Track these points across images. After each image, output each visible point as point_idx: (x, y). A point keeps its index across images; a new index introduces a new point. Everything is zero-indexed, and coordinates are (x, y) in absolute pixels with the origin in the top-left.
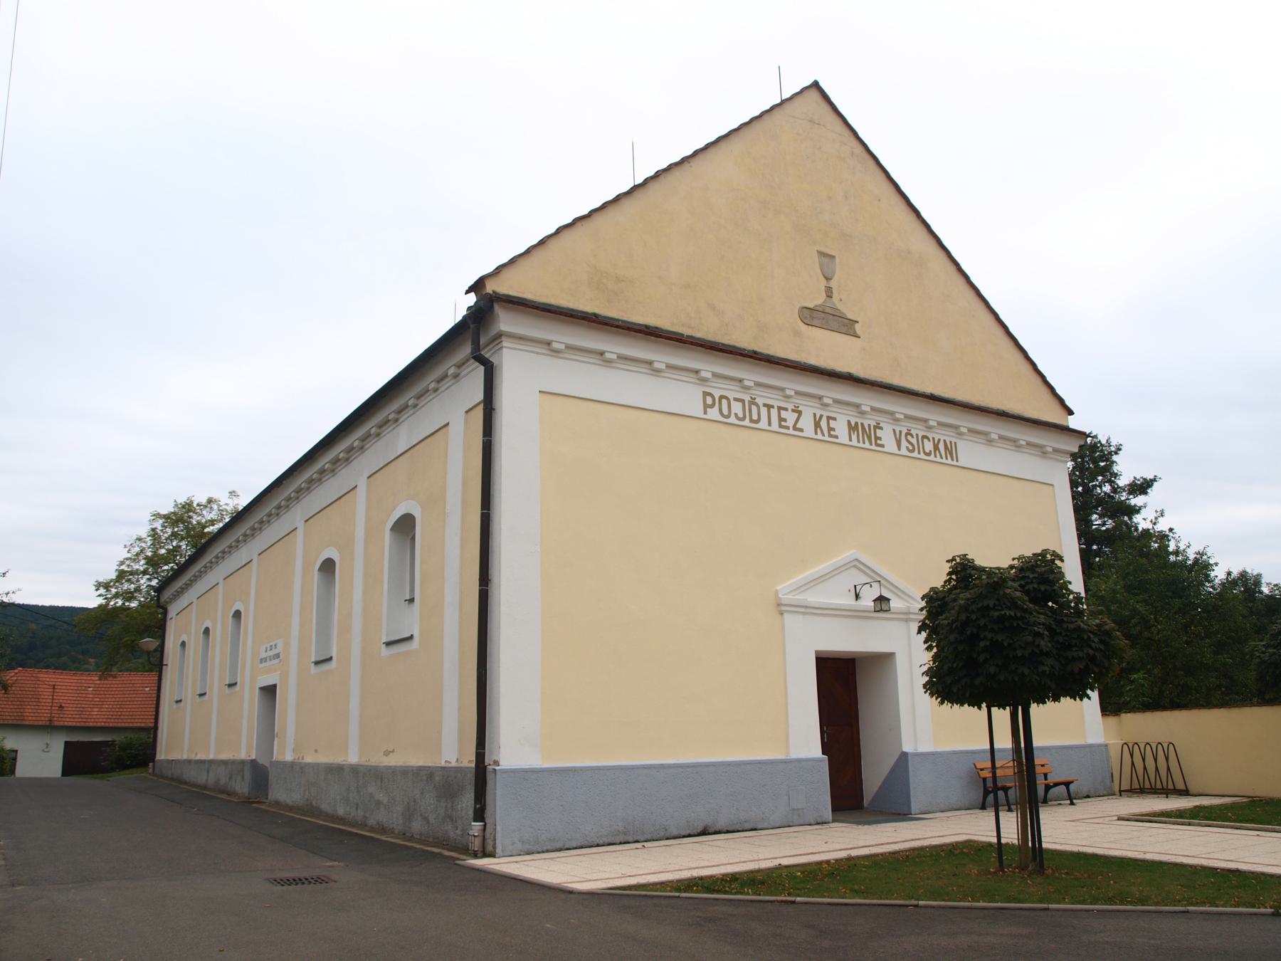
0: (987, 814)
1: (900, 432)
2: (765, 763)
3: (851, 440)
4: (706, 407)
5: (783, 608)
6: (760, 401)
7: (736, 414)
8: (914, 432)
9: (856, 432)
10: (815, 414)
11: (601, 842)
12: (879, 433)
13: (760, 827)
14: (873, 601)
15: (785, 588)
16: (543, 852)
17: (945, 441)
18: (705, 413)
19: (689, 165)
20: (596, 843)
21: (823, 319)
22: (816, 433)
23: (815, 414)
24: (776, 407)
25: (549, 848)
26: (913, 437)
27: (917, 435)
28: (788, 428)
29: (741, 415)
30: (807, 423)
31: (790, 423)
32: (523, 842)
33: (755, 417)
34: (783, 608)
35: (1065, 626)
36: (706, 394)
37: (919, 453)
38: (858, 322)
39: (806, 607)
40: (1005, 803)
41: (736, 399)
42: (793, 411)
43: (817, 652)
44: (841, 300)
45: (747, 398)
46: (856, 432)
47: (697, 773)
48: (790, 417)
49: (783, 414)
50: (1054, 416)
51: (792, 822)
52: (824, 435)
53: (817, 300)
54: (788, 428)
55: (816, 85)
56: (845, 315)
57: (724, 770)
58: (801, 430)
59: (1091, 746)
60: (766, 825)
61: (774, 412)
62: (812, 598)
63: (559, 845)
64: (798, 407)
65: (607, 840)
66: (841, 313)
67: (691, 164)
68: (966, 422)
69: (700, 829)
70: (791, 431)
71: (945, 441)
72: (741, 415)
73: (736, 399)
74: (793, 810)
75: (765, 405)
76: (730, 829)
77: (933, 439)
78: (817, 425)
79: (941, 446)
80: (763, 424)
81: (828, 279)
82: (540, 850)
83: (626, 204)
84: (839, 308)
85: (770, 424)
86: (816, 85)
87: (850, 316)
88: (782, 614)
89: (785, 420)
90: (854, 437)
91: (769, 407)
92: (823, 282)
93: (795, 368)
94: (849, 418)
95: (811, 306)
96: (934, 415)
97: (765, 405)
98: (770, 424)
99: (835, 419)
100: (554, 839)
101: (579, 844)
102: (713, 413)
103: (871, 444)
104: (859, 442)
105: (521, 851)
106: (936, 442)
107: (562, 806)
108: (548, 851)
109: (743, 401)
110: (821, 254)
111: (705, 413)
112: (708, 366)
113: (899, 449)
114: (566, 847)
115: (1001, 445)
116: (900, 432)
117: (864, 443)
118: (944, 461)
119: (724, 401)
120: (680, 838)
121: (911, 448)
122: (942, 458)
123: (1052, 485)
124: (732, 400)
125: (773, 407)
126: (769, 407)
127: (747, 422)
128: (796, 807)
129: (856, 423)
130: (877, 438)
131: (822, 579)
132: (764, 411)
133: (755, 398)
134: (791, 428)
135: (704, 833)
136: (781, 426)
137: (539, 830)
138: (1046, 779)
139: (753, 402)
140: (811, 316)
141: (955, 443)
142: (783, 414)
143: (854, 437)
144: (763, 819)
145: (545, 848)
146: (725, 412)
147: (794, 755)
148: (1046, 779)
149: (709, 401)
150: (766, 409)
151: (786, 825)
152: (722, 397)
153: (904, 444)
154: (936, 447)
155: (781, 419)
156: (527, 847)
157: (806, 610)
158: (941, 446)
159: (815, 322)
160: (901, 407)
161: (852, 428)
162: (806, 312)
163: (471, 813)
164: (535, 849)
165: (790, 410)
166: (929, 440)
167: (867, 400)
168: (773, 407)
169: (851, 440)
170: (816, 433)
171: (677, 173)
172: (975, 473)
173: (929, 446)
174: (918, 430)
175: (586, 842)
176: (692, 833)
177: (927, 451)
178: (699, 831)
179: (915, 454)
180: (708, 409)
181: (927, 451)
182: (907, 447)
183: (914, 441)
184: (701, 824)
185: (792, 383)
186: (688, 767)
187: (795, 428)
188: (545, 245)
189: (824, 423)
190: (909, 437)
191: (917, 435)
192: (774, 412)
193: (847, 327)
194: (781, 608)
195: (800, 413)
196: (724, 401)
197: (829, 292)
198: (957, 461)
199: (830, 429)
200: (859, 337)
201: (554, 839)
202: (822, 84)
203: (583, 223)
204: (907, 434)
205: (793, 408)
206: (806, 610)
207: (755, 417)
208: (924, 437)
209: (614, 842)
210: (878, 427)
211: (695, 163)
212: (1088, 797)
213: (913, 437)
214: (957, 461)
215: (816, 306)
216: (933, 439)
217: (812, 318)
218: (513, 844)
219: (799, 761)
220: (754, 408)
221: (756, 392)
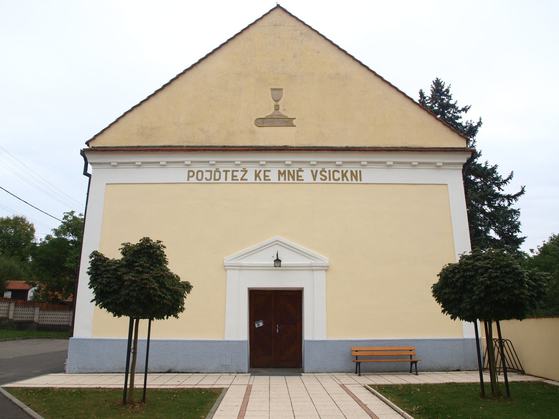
0: (410, 377)
2: (207, 342)
3: (279, 180)
4: (189, 177)
5: (226, 268)
6: (221, 170)
8: (327, 170)
9: (283, 176)
11: (115, 372)
12: (300, 173)
13: (201, 372)
14: (274, 261)
15: (228, 260)
16: (87, 373)
18: (188, 180)
19: (196, 68)
20: (112, 372)
21: (271, 122)
24: (231, 171)
25: (90, 372)
27: (329, 171)
28: (238, 180)
29: (209, 178)
30: (250, 176)
31: (239, 177)
32: (79, 368)
33: (217, 177)
34: (226, 268)
35: (460, 269)
36: (189, 171)
38: (295, 119)
39: (242, 266)
40: (415, 371)
41: (206, 171)
42: (242, 171)
43: (248, 288)
44: (285, 110)
45: (213, 169)
46: (283, 176)
47: (167, 344)
48: (239, 175)
49: (235, 174)
51: (221, 371)
54: (238, 180)
55: (278, 6)
56: (287, 117)
57: (183, 344)
58: (246, 180)
59: (464, 340)
60: (205, 371)
62: (245, 262)
63: (94, 371)
64: (245, 169)
65: (118, 371)
66: (285, 116)
67: (197, 67)
68: (364, 158)
69: (167, 370)
70: (240, 181)
72: (209, 178)
73: (206, 171)
74: (223, 365)
75: (224, 171)
76: (184, 371)
78: (257, 175)
80: (223, 179)
81: (276, 101)
82: (86, 372)
83: (160, 94)
84: (283, 114)
85: (226, 179)
86: (278, 6)
87: (289, 117)
88: (226, 270)
90: (282, 178)
91: (226, 172)
92: (274, 103)
93: (240, 150)
94: (279, 169)
95: (264, 117)
96: (339, 158)
97: (224, 171)
99: (269, 171)
100: (93, 368)
101: (104, 371)
102: (193, 180)
103: (294, 180)
105: (77, 372)
106: (344, 173)
107: (97, 355)
108: (89, 373)
110: (273, 90)
111: (188, 180)
112: (188, 159)
114: (98, 372)
115: (420, 167)
118: (350, 181)
120: (155, 373)
121: (323, 178)
123: (447, 184)
124: (204, 172)
125: (229, 171)
127: (212, 181)
128: (224, 364)
131: (257, 251)
132: (223, 174)
133: (218, 169)
135: (169, 372)
136: (233, 180)
137: (86, 364)
138: (411, 358)
139: (217, 170)
140: (261, 122)
141: (360, 171)
142: (235, 174)
144: (203, 368)
145: (88, 372)
146: (200, 177)
147: (227, 338)
148: (411, 358)
149: (191, 174)
150: (225, 173)
151: (218, 372)
152: (198, 171)
153: (319, 176)
154: (344, 175)
155: (233, 176)
156: (80, 370)
157: (241, 268)
159: (265, 124)
160: (313, 158)
162: (260, 121)
164: (83, 371)
165: (240, 171)
167: (288, 158)
168: (229, 171)
169: (279, 180)
170: (256, 180)
171: (189, 73)
172: (377, 185)
173: (338, 175)
174: (330, 168)
175: (107, 371)
176: (162, 371)
178: (166, 371)
179: (327, 181)
180: (190, 178)
181: (336, 178)
183: (327, 175)
184: (168, 368)
185: (238, 158)
186: (162, 341)
188: (118, 122)
189: (262, 175)
190: (323, 173)
191: (329, 171)
192: (229, 175)
193: (288, 122)
194: (225, 268)
196: (200, 174)
197: (277, 108)
198: (361, 180)
200: (295, 126)
201: (93, 368)
203: (137, 109)
204: (321, 172)
205: (215, 170)
206: (241, 268)
207: (217, 177)
209: (121, 372)
211: (200, 66)
212: (458, 370)
215: (267, 116)
217: (263, 122)
218: (74, 368)
219: (228, 342)
220: (217, 174)
221: (218, 166)
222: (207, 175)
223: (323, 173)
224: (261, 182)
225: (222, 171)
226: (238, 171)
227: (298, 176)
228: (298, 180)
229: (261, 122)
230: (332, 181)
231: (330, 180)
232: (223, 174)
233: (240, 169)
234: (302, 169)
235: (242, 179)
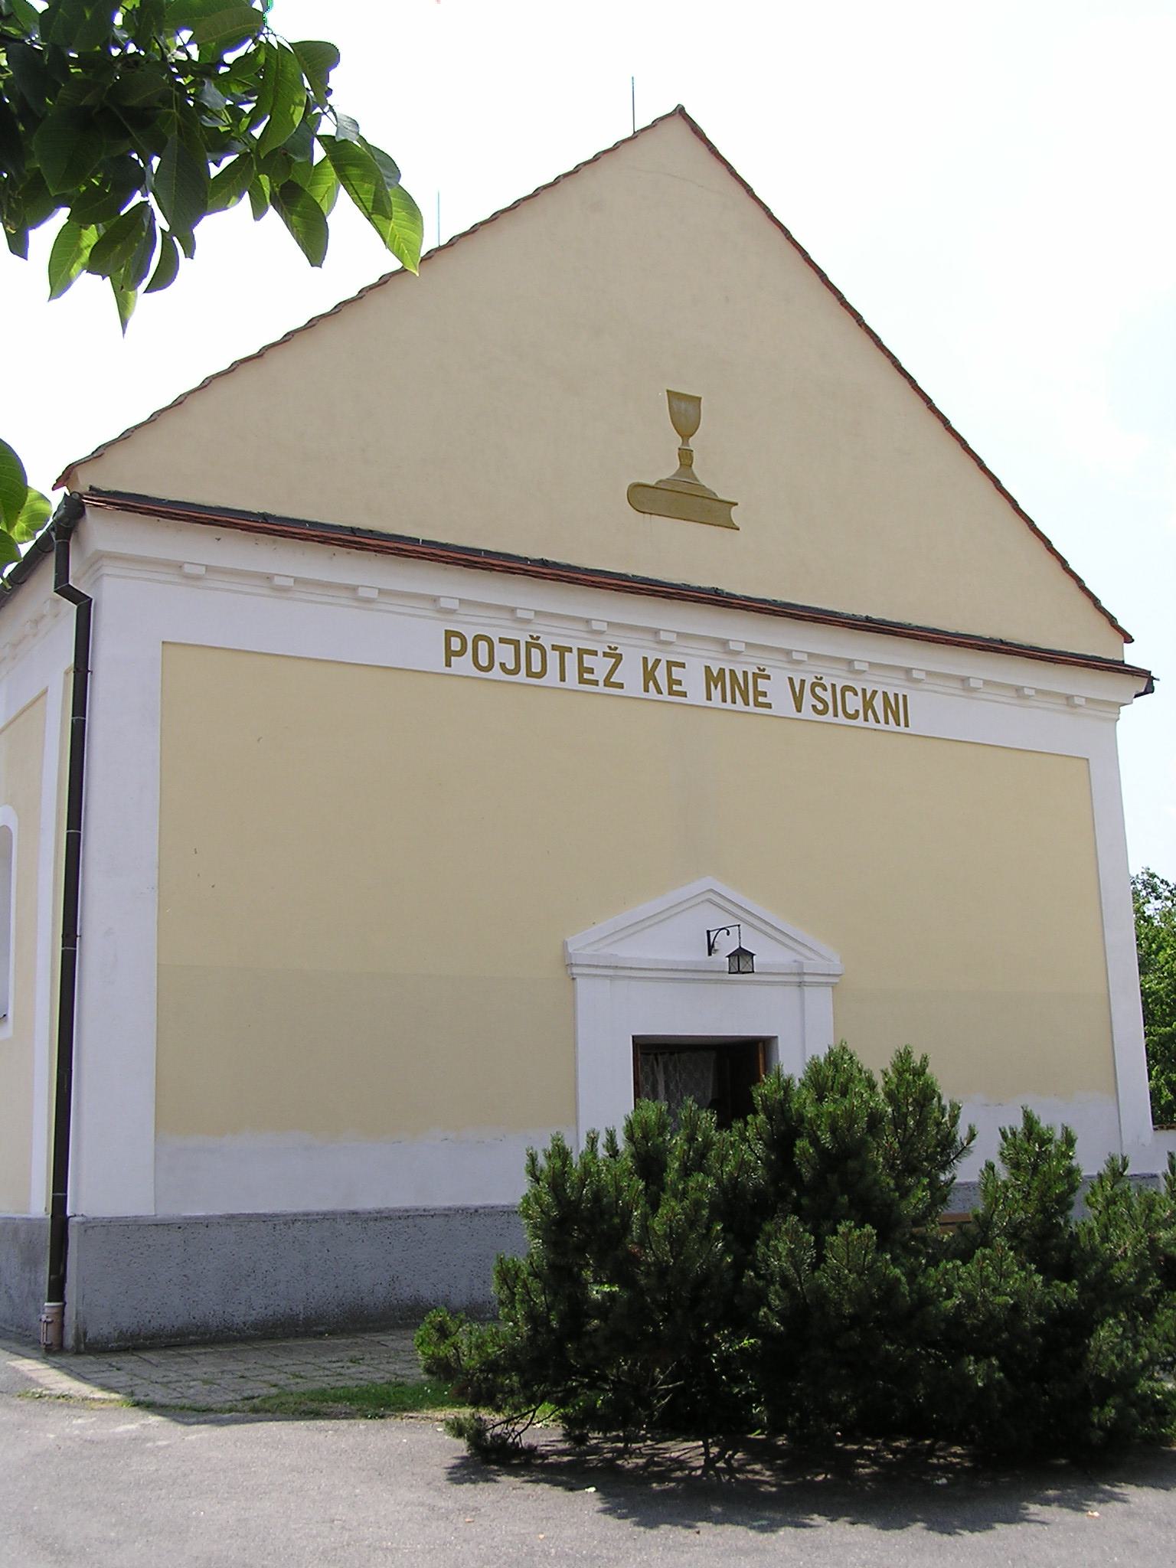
1: (803, 682)
3: (709, 698)
4: (450, 654)
6: (546, 642)
7: (502, 665)
10: (645, 659)
17: (885, 693)
18: (448, 664)
22: (646, 690)
23: (645, 659)
24: (575, 651)
26: (825, 689)
27: (833, 686)
28: (596, 683)
29: (511, 666)
30: (630, 675)
31: (600, 675)
33: (536, 668)
36: (449, 634)
37: (836, 715)
38: (736, 504)
41: (502, 640)
42: (605, 654)
45: (524, 638)
48: (601, 666)
50: (1096, 643)
52: (660, 692)
53: (663, 468)
54: (596, 683)
55: (680, 111)
58: (621, 686)
61: (571, 659)
62: (630, 952)
64: (616, 648)
71: (885, 693)
72: (511, 666)
73: (502, 640)
75: (554, 648)
77: (864, 690)
78: (649, 676)
79: (878, 703)
80: (552, 677)
85: (563, 679)
86: (680, 111)
87: (721, 496)
88: (574, 979)
89: (591, 671)
90: (716, 693)
97: (554, 648)
98: (563, 679)
99: (682, 665)
102: (463, 665)
103: (747, 704)
104: (724, 700)
109: (516, 643)
111: (448, 664)
113: (799, 711)
116: (803, 682)
117: (734, 702)
118: (882, 726)
119: (483, 646)
121: (820, 707)
122: (878, 721)
124: (496, 641)
125: (570, 650)
126: (563, 650)
129: (722, 671)
130: (759, 693)
132: (553, 657)
134: (601, 683)
136: (582, 681)
141: (905, 697)
143: (716, 693)
146: (484, 661)
152: (477, 638)
153: (808, 700)
154: (868, 705)
155: (582, 669)
158: (878, 703)
161: (713, 679)
163: (45, 1289)
165: (600, 654)
166: (856, 694)
168: (570, 650)
169: (709, 698)
170: (646, 690)
173: (854, 703)
177: (851, 712)
179: (829, 717)
182: (814, 707)
183: (827, 696)
187: (608, 683)
189: (661, 674)
190: (818, 690)
191: (833, 686)
192: (571, 659)
195: (619, 658)
196: (483, 646)
198: (907, 725)
199: (672, 681)
200: (738, 529)
202: (688, 111)
207: (536, 668)
208: (845, 689)
210: (761, 675)
213: (825, 689)
214: (907, 725)
216: (864, 690)
220: (536, 653)
222: (505, 654)
223: (818, 690)
224: (709, 704)
225: (548, 649)
226: (595, 653)
228: (757, 704)
229: (642, 498)
230: (841, 719)
231: (836, 715)
232: (553, 657)
233: (601, 648)
234: (765, 673)
235: (608, 683)
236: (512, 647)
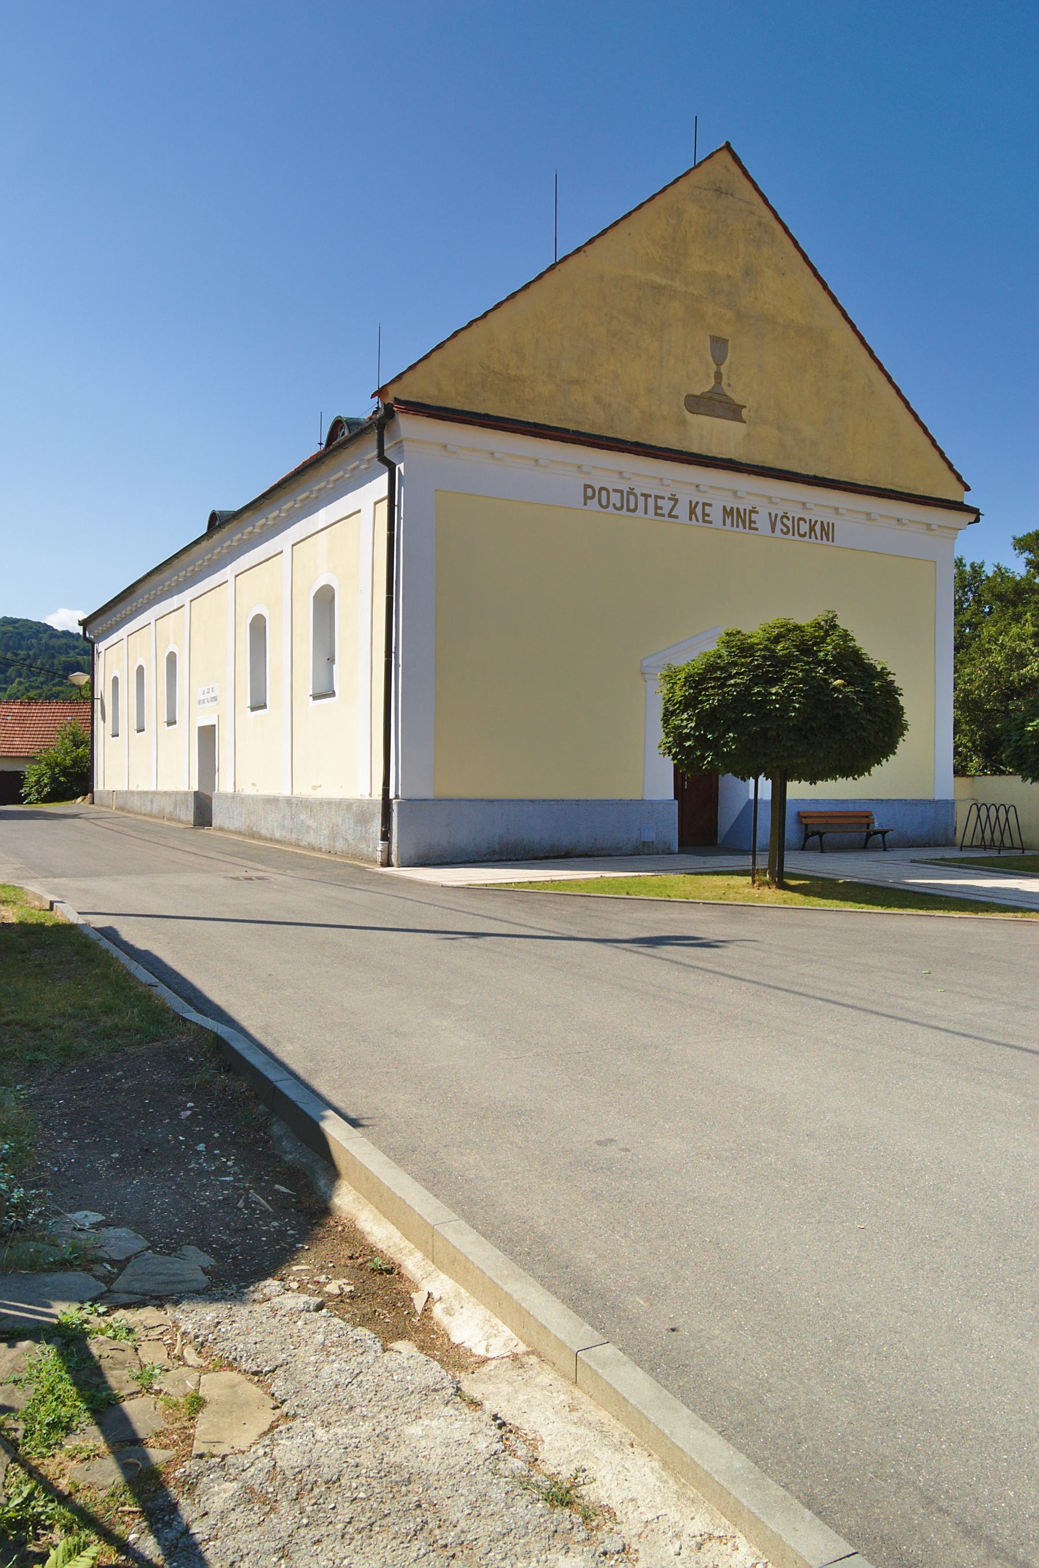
1: (776, 515)
3: (724, 524)
7: (614, 505)
10: (691, 502)
12: (754, 516)
17: (822, 522)
18: (585, 504)
22: (691, 519)
23: (691, 502)
24: (653, 497)
26: (788, 519)
27: (793, 518)
28: (663, 515)
29: (618, 505)
30: (682, 510)
33: (632, 507)
36: (586, 486)
37: (793, 534)
38: (745, 407)
41: (614, 490)
42: (669, 499)
45: (626, 489)
48: (666, 505)
49: (660, 502)
52: (697, 521)
53: (703, 386)
54: (663, 515)
58: (676, 517)
61: (651, 501)
71: (822, 522)
73: (614, 490)
75: (642, 495)
77: (810, 520)
78: (692, 511)
79: (818, 528)
84: (728, 394)
85: (646, 513)
89: (661, 508)
90: (728, 521)
97: (642, 495)
98: (646, 513)
99: (710, 505)
104: (732, 526)
109: (622, 492)
111: (585, 504)
113: (773, 532)
116: (776, 515)
117: (738, 527)
119: (604, 493)
121: (785, 530)
122: (817, 538)
124: (611, 491)
125: (650, 496)
126: (646, 496)
129: (732, 509)
130: (751, 522)
132: (641, 500)
134: (666, 515)
136: (656, 514)
140: (697, 404)
141: (833, 524)
142: (660, 502)
143: (728, 521)
149: (590, 492)
150: (643, 498)
152: (602, 489)
154: (812, 529)
155: (657, 507)
158: (818, 528)
161: (727, 512)
163: (379, 834)
165: (666, 499)
166: (806, 522)
168: (650, 496)
169: (724, 524)
170: (691, 519)
173: (804, 528)
177: (802, 533)
181: (802, 533)
182: (782, 530)
183: (789, 524)
187: (670, 515)
189: (699, 510)
190: (785, 520)
191: (793, 518)
192: (651, 501)
193: (734, 412)
195: (676, 501)
196: (604, 493)
197: (718, 376)
198: (833, 541)
199: (704, 515)
202: (732, 146)
204: (782, 517)
207: (632, 507)
208: (800, 519)
210: (754, 511)
213: (788, 519)
214: (833, 541)
216: (810, 520)
220: (632, 497)
222: (615, 498)
223: (785, 520)
225: (639, 495)
226: (663, 498)
227: (751, 522)
228: (750, 528)
230: (796, 536)
231: (793, 534)
232: (641, 500)
233: (667, 495)
235: (670, 515)
236: (619, 494)
